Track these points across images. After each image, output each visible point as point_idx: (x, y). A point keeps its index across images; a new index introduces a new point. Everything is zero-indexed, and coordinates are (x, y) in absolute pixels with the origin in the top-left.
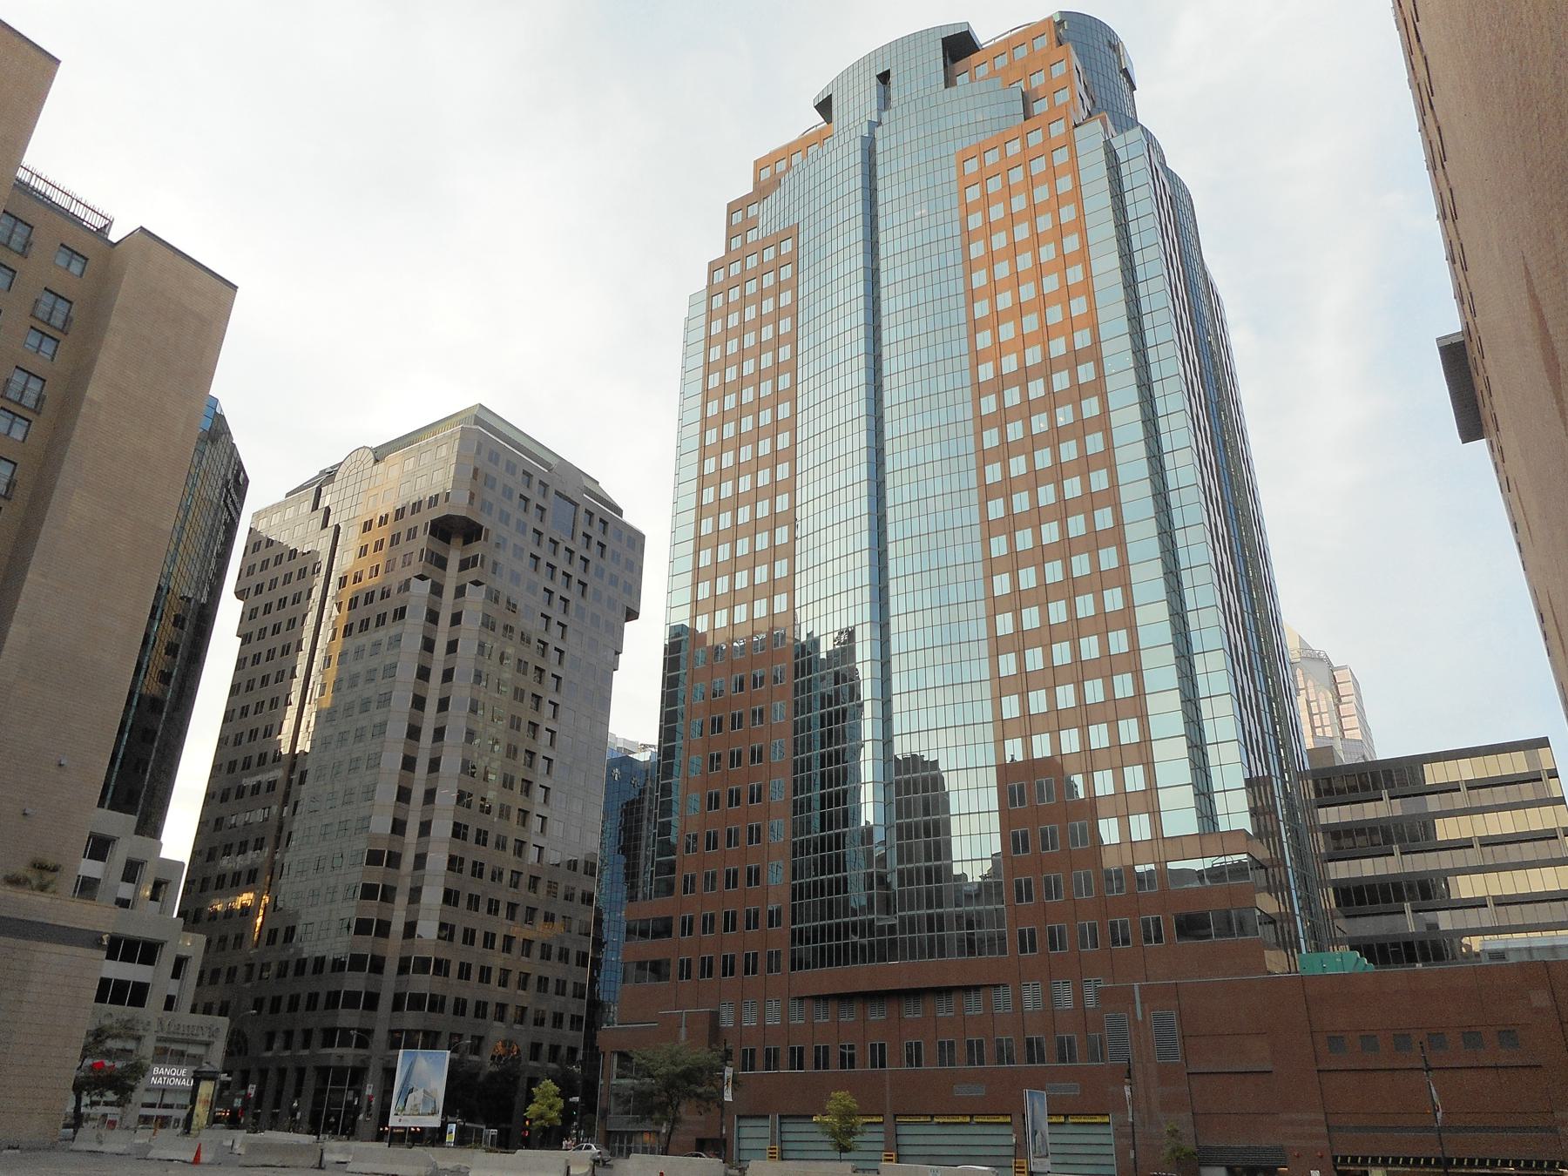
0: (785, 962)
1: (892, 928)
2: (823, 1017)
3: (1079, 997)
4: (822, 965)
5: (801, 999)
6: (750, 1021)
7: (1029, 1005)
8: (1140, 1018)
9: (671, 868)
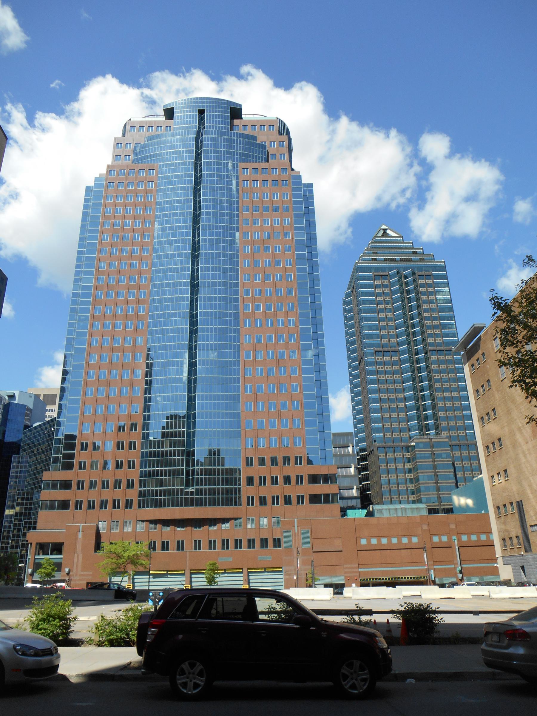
0: (135, 504)
1: (192, 493)
2: (156, 529)
3: (270, 524)
4: (156, 506)
5: (143, 521)
6: (115, 529)
7: (249, 526)
8: (296, 531)
9: (72, 456)
